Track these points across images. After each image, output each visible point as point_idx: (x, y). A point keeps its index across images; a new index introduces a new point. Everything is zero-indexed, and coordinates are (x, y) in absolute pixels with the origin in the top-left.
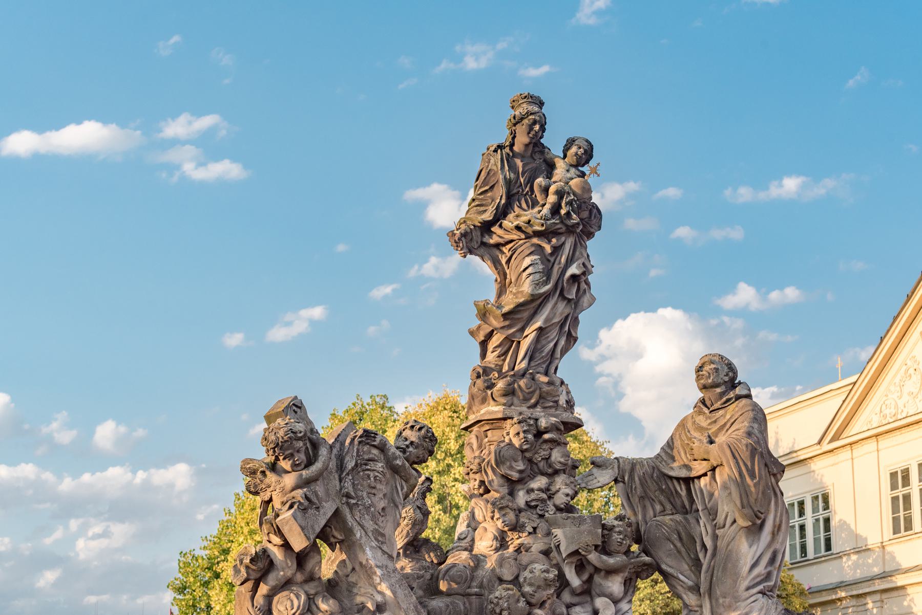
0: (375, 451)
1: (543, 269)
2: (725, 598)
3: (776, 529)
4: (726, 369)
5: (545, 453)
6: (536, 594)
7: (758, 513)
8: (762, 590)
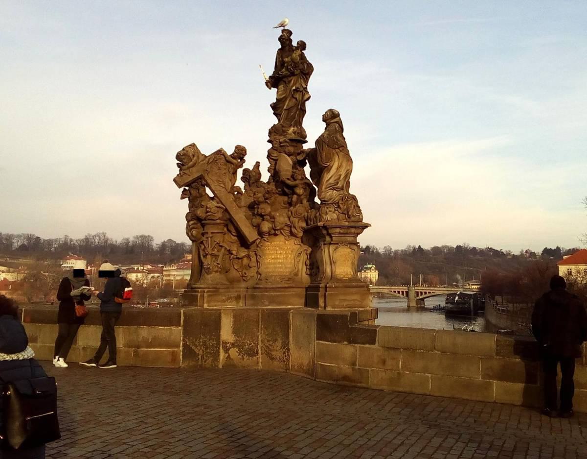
0: (222, 156)
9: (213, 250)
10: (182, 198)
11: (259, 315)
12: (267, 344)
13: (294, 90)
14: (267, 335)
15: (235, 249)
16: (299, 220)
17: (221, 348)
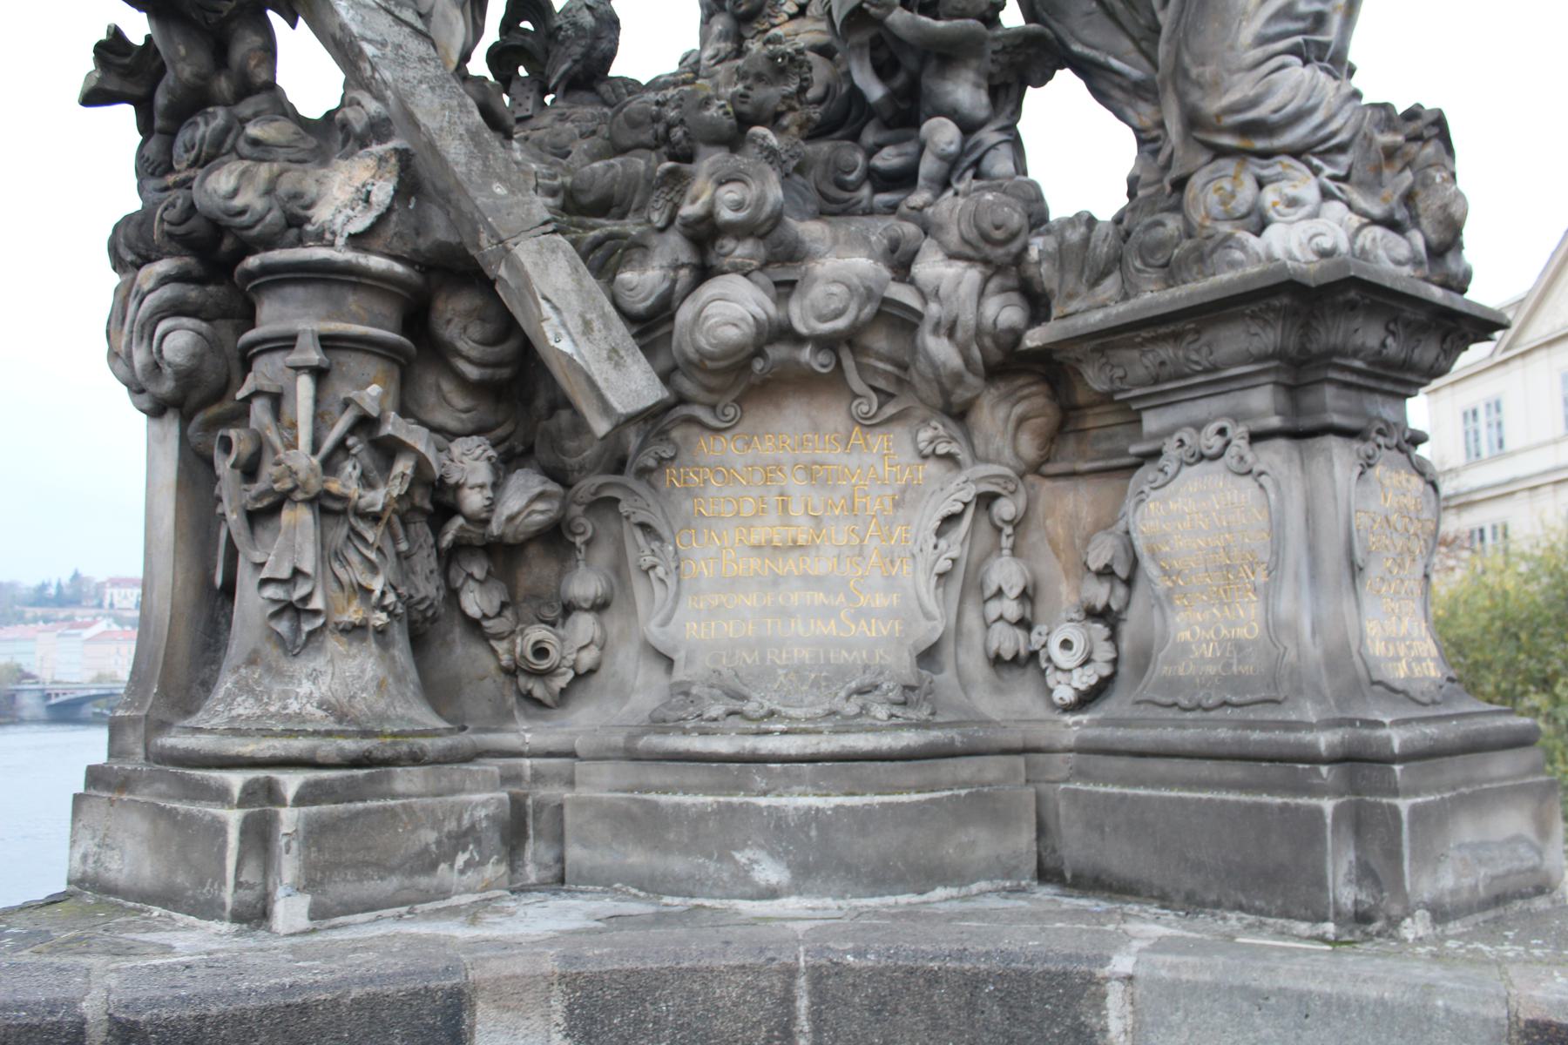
2: (1203, 64)
6: (750, 93)
8: (1298, 45)
9: (329, 465)
11: (788, 1000)
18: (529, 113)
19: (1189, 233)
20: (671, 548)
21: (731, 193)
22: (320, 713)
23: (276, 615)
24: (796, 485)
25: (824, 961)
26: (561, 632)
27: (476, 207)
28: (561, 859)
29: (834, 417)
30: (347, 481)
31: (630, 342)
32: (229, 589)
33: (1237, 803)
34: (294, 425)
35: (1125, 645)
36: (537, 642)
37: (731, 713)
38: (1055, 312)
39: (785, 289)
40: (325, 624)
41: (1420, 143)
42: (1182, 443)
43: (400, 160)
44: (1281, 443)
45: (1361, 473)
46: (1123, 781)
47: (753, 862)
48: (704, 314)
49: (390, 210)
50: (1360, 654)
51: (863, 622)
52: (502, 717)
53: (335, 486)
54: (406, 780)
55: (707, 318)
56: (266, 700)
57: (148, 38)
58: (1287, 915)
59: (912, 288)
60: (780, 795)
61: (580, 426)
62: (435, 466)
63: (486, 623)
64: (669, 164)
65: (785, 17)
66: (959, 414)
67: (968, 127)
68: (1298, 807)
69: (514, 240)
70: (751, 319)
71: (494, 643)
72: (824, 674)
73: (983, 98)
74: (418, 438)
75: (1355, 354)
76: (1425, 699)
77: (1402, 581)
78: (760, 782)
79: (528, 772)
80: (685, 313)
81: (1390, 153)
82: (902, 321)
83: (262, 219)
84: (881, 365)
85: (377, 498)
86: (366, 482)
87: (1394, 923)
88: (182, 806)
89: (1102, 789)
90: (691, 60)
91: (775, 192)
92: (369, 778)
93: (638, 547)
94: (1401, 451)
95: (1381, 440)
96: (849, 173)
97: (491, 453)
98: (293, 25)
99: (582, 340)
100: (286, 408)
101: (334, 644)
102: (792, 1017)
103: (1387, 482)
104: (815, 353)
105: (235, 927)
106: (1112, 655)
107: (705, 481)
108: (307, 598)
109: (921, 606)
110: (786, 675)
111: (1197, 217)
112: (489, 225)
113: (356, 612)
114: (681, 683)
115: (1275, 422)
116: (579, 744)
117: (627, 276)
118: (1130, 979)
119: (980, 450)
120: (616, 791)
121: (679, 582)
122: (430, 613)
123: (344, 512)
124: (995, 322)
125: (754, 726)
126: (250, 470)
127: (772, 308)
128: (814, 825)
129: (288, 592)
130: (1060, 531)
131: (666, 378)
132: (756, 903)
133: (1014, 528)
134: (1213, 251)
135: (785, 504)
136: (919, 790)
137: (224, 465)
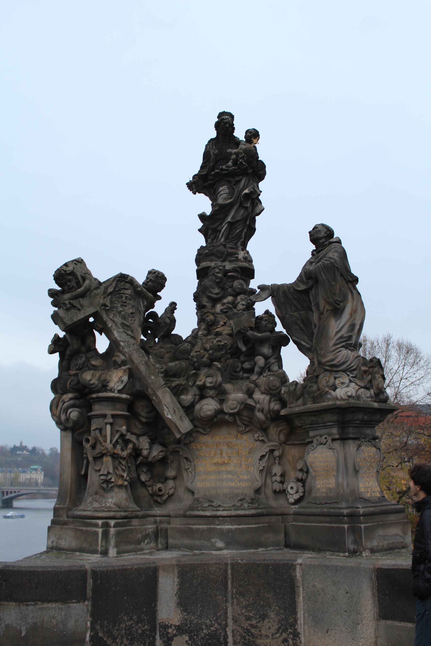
0: (128, 285)
1: (229, 192)
2: (321, 350)
3: (353, 312)
4: (325, 230)
5: (230, 284)
6: (214, 354)
7: (336, 301)
9: (115, 446)
10: (51, 352)
11: (226, 571)
12: (246, 625)
13: (246, 194)
14: (246, 607)
15: (147, 446)
16: (271, 399)
17: (158, 637)
18: (152, 345)
19: (319, 389)
20: (193, 464)
21: (209, 380)
22: (114, 506)
23: (103, 483)
24: (225, 448)
25: (234, 562)
26: (165, 485)
27: (148, 383)
28: (167, 543)
29: (234, 431)
30: (118, 450)
31: (184, 414)
32: (86, 476)
33: (328, 526)
34: (105, 436)
35: (307, 488)
36: (159, 488)
37: (209, 506)
38: (288, 406)
39: (222, 402)
40: (114, 485)
41: (373, 368)
42: (317, 440)
43: (129, 371)
44: (339, 442)
45: (357, 449)
46: (304, 522)
47: (216, 542)
48: (202, 408)
49: (127, 383)
50: (357, 491)
51: (241, 482)
52: (150, 507)
53: (116, 452)
54: (135, 522)
55: (203, 409)
56: (101, 503)
57: (64, 336)
58: (338, 551)
59: (253, 400)
60: (222, 525)
61: (170, 432)
62: (137, 445)
63: (146, 483)
64: (194, 371)
65: (220, 326)
66: (264, 430)
67: (266, 358)
68: (340, 527)
69: (157, 391)
70: (214, 409)
71: (148, 488)
72: (232, 496)
73: (271, 351)
74: (133, 438)
75: (356, 420)
76: (374, 502)
77: (370, 473)
78: (217, 522)
79: (158, 521)
80: (197, 407)
81: (365, 372)
82: (250, 409)
83: (97, 386)
84: (245, 418)
85: (125, 454)
86: (122, 450)
87: (361, 553)
88: (84, 528)
89: (299, 524)
90: (195, 332)
91: (220, 379)
92: (127, 521)
93: (184, 463)
94: (369, 442)
95: (363, 440)
96: (238, 368)
97: (149, 441)
98: (101, 335)
99: (173, 415)
100: (103, 432)
101: (116, 490)
102: (227, 574)
103: (365, 450)
104: (229, 417)
105: (101, 556)
106: (303, 491)
107: (201, 447)
108: (111, 479)
109: (256, 478)
110: (222, 496)
111: (320, 386)
112: (151, 387)
113: (121, 482)
114: (197, 498)
115: (337, 437)
116: (171, 513)
117: (183, 397)
118: (301, 564)
119: (270, 438)
120: (181, 525)
121: (195, 472)
122: (134, 481)
123: (118, 458)
124: (273, 408)
125: (215, 509)
126: (94, 447)
127: (219, 406)
128: (230, 533)
129: (106, 477)
130: (291, 459)
131: (192, 421)
132: (217, 552)
133: (279, 458)
134: (324, 395)
135: (221, 453)
136: (255, 524)
137: (87, 446)
